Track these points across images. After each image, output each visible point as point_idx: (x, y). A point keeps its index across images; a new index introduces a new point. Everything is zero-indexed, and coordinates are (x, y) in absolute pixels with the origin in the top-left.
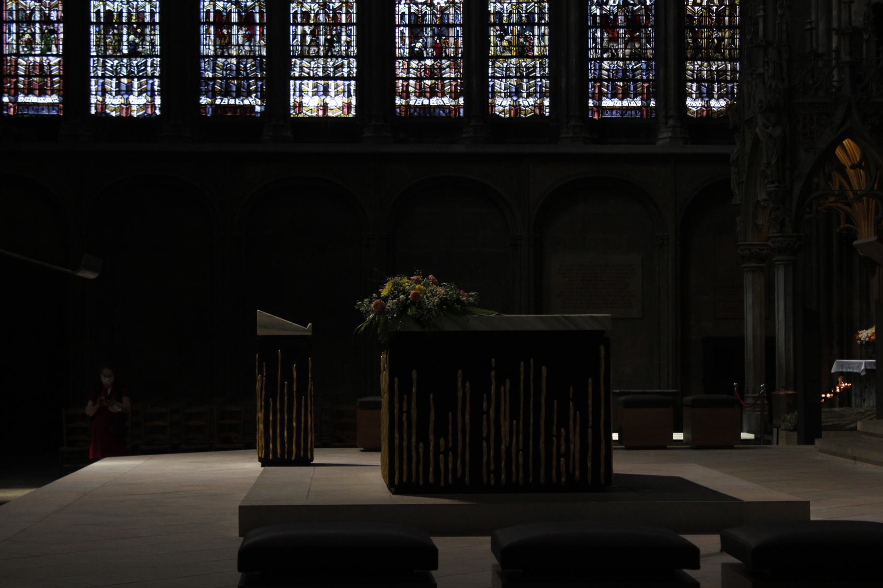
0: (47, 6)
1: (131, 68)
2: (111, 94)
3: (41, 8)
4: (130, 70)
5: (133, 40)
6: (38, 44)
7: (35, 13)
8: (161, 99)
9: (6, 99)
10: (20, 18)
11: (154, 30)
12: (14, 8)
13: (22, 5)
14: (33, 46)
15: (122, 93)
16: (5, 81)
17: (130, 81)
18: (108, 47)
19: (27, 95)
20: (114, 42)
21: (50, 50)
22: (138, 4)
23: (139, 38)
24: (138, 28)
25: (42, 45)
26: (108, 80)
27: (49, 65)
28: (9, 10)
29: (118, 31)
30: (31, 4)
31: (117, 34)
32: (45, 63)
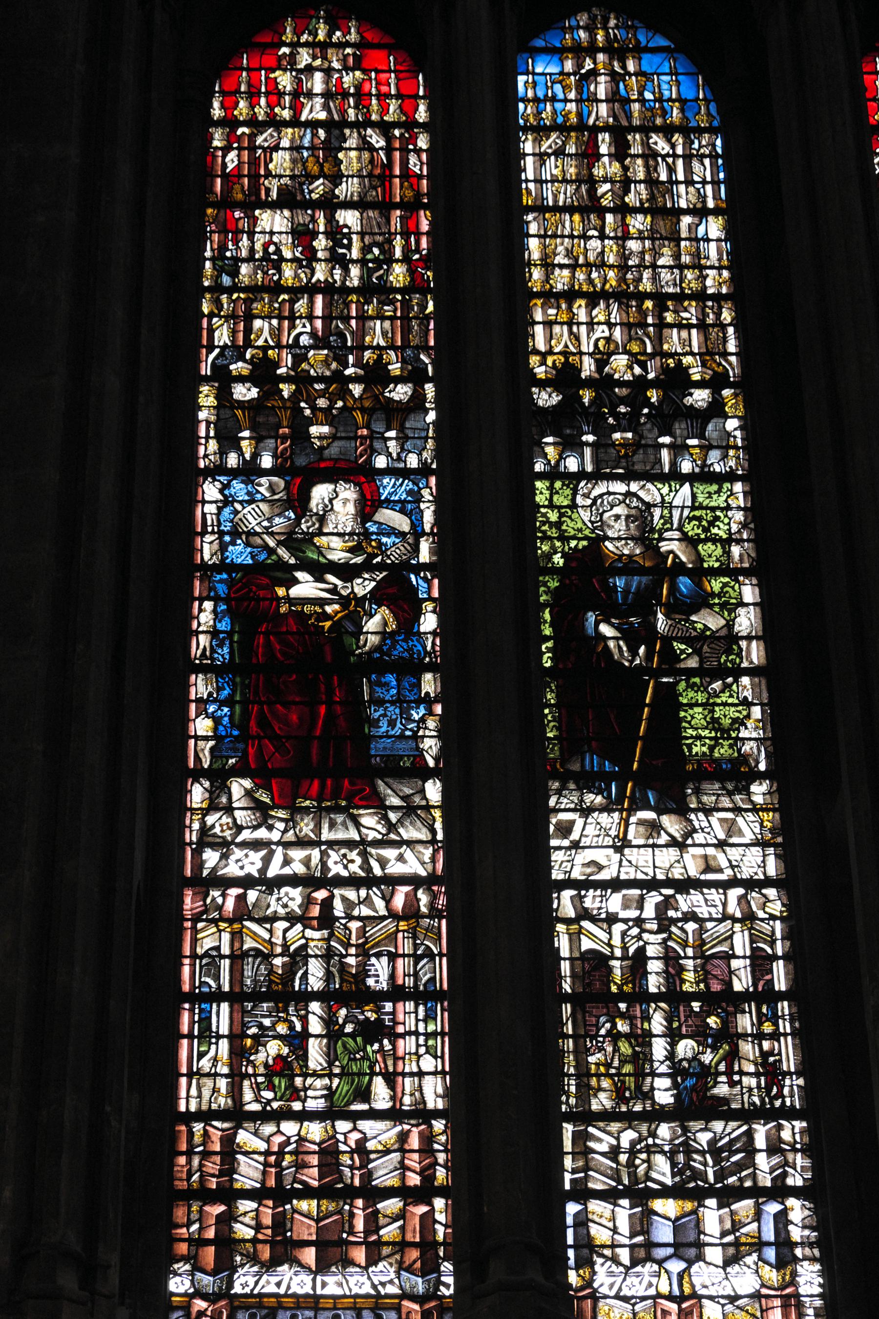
0: (353, 941)
1: (689, 1158)
2: (615, 1260)
3: (329, 948)
4: (687, 1166)
5: (690, 1055)
6: (315, 1074)
7: (306, 964)
8: (823, 1273)
9: (179, 1285)
10: (248, 982)
11: (774, 1019)
12: (226, 950)
13: (255, 936)
14: (298, 1081)
15: (661, 1253)
16: (180, 1214)
17: (689, 1206)
18: (594, 1082)
19: (270, 1265)
20: (616, 1063)
21: (365, 1095)
22: (702, 930)
23: (715, 1049)
24: (706, 1013)
25: (331, 1076)
26: (596, 1206)
27: (360, 1148)
28: (206, 954)
29: (632, 1026)
30: (290, 935)
31: (627, 1036)
32: (345, 1143)
